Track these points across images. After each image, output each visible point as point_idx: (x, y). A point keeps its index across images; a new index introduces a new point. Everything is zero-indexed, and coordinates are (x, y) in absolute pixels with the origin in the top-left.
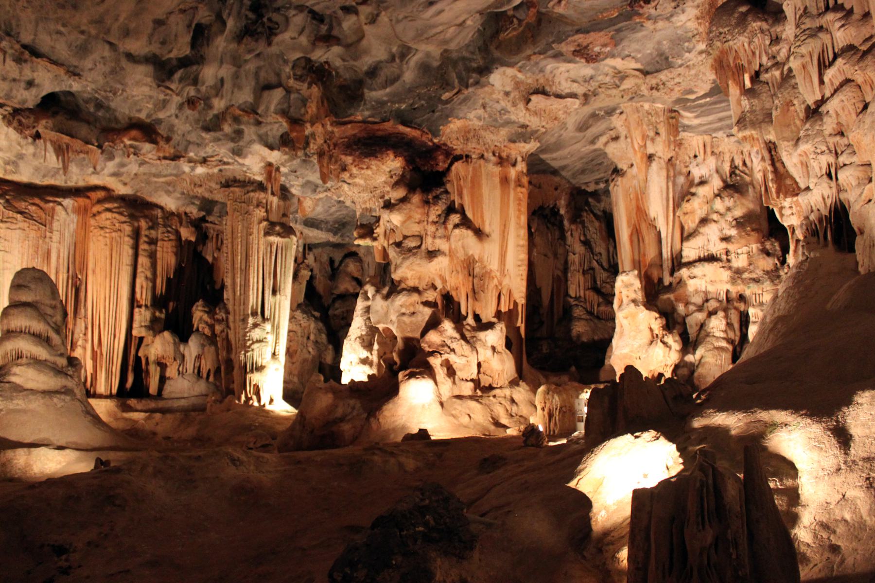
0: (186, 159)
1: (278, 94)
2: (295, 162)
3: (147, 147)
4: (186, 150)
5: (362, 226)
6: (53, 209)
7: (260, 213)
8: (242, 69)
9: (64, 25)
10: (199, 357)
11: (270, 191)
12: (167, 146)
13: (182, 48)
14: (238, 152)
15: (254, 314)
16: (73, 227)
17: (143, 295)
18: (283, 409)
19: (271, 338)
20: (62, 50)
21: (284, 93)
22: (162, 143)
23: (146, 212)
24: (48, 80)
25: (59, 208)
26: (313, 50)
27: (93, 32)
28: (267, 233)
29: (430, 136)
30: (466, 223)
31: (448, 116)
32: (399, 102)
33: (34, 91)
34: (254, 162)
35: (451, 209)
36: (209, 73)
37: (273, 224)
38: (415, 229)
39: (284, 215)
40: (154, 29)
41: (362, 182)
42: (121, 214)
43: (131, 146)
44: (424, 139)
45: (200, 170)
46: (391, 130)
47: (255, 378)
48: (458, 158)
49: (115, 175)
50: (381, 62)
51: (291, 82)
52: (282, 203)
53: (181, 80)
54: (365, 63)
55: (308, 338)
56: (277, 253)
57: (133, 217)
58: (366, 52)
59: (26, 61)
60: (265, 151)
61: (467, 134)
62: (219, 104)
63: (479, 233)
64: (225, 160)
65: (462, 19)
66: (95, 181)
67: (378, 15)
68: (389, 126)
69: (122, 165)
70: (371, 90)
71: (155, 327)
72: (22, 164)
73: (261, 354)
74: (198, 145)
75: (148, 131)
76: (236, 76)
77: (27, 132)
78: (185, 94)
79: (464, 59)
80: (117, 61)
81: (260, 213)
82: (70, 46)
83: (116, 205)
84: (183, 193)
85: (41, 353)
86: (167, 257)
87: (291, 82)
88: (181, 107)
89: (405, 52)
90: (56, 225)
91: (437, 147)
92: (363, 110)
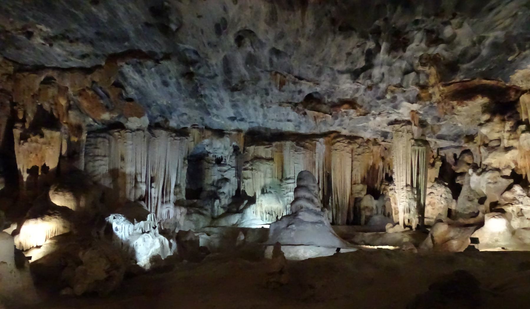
0: (371, 114)
1: (413, 75)
2: (425, 108)
3: (352, 111)
4: (370, 110)
5: (467, 136)
6: (315, 144)
8: (393, 67)
9: (310, 64)
11: (413, 124)
12: (361, 110)
13: (361, 63)
14: (395, 107)
16: (324, 150)
20: (311, 76)
21: (416, 74)
22: (358, 108)
23: (356, 141)
24: (307, 88)
25: (317, 143)
26: (428, 50)
27: (321, 64)
29: (503, 82)
31: (514, 69)
32: (481, 67)
33: (301, 95)
36: (376, 72)
37: (416, 140)
39: (423, 135)
40: (347, 57)
41: (464, 113)
42: (344, 142)
43: (345, 112)
44: (500, 84)
45: (378, 119)
46: (477, 84)
48: (524, 92)
49: (339, 125)
50: (467, 48)
52: (421, 130)
53: (364, 77)
55: (441, 196)
58: (459, 44)
59: (297, 83)
60: (409, 105)
62: (383, 86)
64: (390, 112)
65: (514, 12)
66: (332, 129)
67: (463, 23)
68: (476, 82)
69: (342, 121)
70: (463, 63)
72: (301, 126)
74: (376, 107)
75: (352, 104)
76: (390, 71)
77: (301, 113)
78: (366, 84)
79: (521, 33)
80: (334, 74)
82: (313, 72)
83: (342, 139)
84: (371, 130)
88: (365, 90)
89: (481, 40)
90: (317, 151)
91: (509, 88)
92: (459, 76)
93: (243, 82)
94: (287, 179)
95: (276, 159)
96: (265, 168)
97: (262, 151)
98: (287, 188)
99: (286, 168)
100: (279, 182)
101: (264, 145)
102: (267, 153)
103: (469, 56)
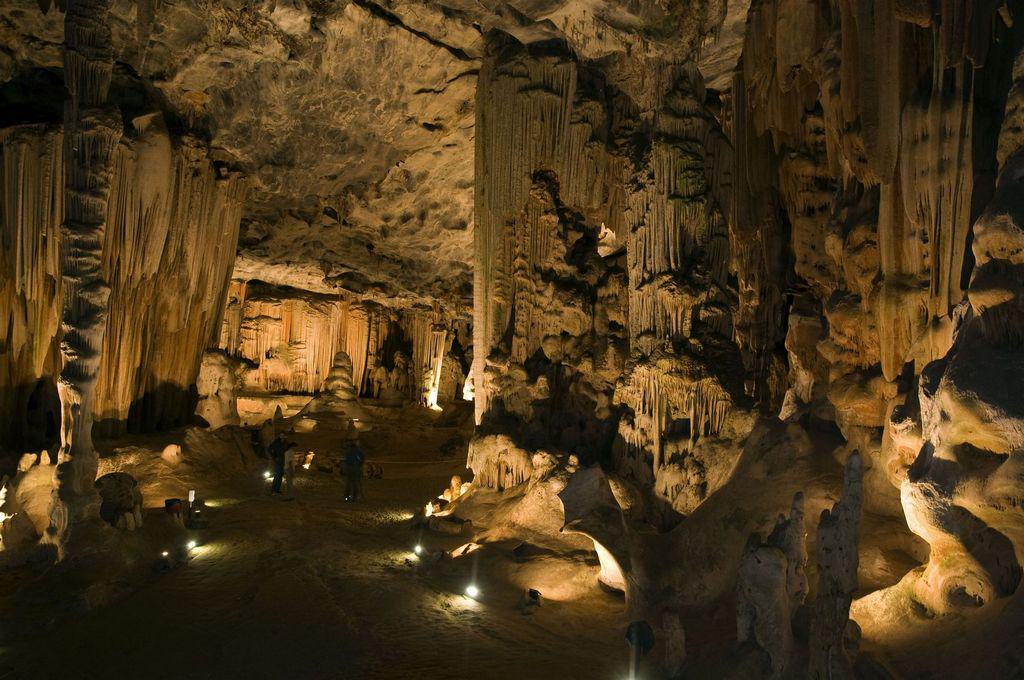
7: (430, 321)
10: (398, 379)
15: (426, 366)
17: (373, 350)
18: (436, 408)
19: (432, 377)
24: (344, 271)
28: (433, 330)
34: (428, 300)
37: (435, 326)
47: (426, 394)
56: (437, 339)
57: (369, 312)
71: (377, 364)
73: (429, 384)
75: (382, 287)
81: (430, 321)
85: (346, 385)
86: (384, 330)
93: (288, 263)
94: (296, 343)
95: (284, 319)
96: (271, 327)
97: (270, 309)
98: (296, 354)
99: (294, 329)
100: (287, 346)
101: (271, 301)
102: (275, 312)
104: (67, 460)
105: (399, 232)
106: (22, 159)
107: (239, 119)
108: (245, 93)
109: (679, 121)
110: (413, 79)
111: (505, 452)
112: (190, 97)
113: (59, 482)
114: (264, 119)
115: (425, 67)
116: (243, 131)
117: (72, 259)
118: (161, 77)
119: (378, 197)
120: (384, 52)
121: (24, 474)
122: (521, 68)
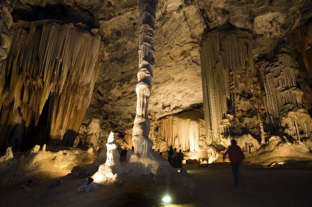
30: (126, 142)
35: (124, 140)
38: (119, 142)
48: (126, 134)
51: (107, 123)
54: (118, 124)
58: (119, 123)
61: (128, 132)
63: (128, 144)
87: (107, 123)
89: (124, 125)
103: (120, 126)
104: (143, 121)
105: (126, 98)
106: (52, 30)
107: (120, 41)
108: (128, 32)
109: (288, 50)
110: (178, 40)
111: (251, 140)
112: (106, 31)
113: (142, 131)
114: (129, 43)
115: (182, 37)
116: (119, 46)
117: (148, 36)
118: (103, 19)
119: (128, 84)
120: (178, 28)
121: (35, 154)
122: (239, 32)
